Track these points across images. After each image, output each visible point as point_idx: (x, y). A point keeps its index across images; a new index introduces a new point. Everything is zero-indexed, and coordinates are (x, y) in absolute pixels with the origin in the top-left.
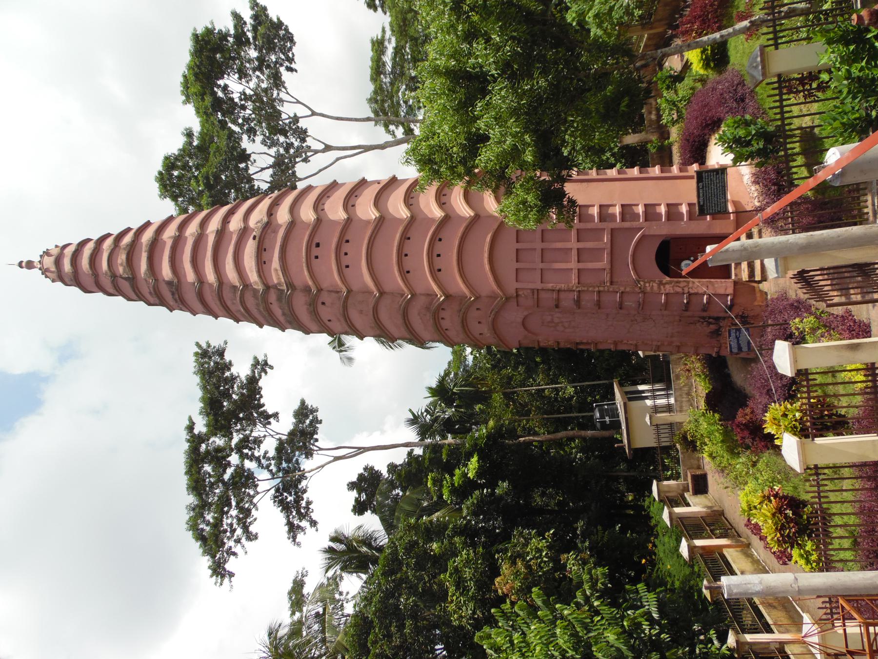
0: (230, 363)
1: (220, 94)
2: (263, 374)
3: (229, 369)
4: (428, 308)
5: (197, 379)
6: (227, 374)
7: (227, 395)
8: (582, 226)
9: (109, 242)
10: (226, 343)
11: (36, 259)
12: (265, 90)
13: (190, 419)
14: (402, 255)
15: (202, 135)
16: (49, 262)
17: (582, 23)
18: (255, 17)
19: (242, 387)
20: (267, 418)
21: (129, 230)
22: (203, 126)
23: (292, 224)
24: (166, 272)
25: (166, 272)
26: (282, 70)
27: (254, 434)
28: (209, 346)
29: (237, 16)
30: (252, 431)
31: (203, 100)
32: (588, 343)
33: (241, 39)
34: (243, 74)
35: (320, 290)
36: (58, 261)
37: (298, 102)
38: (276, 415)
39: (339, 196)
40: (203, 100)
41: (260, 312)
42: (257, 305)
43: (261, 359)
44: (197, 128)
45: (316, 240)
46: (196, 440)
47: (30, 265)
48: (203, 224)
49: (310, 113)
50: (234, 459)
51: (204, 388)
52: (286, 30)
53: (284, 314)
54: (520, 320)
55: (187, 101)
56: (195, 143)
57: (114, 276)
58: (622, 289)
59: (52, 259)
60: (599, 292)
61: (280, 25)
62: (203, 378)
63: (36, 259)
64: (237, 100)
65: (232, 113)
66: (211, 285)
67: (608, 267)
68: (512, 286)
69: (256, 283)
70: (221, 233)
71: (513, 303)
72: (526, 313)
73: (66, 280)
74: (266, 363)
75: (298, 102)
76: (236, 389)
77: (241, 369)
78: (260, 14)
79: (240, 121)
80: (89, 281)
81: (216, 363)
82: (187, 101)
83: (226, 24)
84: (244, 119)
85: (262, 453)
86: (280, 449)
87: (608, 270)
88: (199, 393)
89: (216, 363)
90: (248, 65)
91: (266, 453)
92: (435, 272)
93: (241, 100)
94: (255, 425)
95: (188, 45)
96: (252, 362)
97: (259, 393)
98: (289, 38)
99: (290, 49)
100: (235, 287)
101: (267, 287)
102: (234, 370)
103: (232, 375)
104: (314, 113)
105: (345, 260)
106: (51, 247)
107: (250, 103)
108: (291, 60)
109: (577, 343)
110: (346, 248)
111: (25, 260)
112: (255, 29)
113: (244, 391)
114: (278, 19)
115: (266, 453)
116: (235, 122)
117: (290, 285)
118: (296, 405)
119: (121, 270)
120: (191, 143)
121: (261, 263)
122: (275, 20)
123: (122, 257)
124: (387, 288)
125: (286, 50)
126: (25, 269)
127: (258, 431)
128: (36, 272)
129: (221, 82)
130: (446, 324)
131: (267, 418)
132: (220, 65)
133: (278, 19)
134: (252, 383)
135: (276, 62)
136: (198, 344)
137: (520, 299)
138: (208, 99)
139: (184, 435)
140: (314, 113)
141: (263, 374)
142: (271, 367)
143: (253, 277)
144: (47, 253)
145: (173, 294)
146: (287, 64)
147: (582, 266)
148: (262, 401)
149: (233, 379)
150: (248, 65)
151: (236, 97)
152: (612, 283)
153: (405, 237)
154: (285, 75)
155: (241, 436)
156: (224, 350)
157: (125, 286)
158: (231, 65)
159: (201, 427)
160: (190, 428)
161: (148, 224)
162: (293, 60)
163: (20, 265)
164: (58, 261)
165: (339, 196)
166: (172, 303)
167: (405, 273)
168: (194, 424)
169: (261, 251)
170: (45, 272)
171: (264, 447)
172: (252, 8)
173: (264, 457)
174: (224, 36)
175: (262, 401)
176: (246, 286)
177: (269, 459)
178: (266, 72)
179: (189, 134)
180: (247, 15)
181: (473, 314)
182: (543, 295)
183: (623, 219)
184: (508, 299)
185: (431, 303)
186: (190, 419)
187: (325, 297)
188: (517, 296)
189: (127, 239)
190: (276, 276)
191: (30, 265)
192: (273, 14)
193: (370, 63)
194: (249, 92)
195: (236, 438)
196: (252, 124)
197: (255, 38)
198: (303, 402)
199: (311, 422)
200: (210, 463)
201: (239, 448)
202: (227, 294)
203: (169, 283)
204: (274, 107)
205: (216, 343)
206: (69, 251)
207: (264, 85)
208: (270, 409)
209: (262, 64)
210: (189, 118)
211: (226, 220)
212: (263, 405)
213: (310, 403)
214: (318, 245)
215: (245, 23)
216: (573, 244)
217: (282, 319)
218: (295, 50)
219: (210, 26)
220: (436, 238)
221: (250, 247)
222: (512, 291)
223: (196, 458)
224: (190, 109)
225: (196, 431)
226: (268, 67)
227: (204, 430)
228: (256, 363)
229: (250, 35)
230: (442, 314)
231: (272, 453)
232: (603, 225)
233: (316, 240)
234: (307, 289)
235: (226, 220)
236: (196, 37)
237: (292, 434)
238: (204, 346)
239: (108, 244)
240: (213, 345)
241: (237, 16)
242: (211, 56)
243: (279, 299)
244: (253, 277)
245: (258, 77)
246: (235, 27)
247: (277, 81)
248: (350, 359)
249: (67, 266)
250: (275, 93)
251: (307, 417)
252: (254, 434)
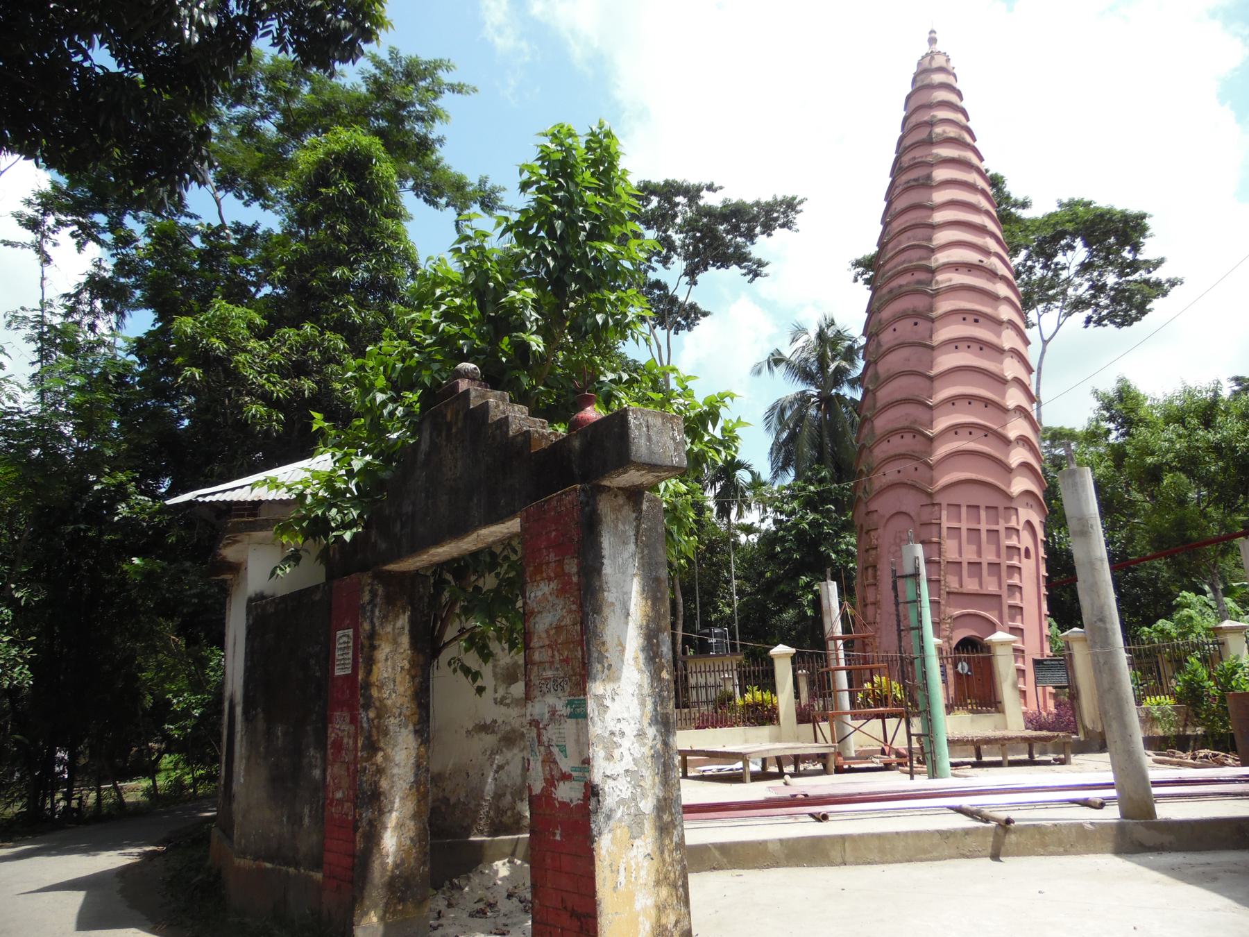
0: (769, 235)
1: (1063, 242)
2: (744, 271)
3: (763, 233)
4: (915, 422)
5: (766, 198)
6: (758, 230)
7: (735, 229)
8: (1004, 568)
9: (959, 117)
10: (797, 231)
11: (938, 47)
12: (1064, 292)
13: (721, 188)
14: (970, 398)
15: (1019, 220)
16: (939, 61)
17: (1181, 606)
18: (1158, 284)
19: (737, 247)
20: (691, 273)
21: (975, 140)
22: (1033, 221)
23: (995, 298)
24: (940, 174)
25: (940, 174)
26: (1089, 312)
27: (675, 257)
28: (797, 212)
29: (1159, 263)
30: (679, 255)
31: (1069, 221)
32: (875, 577)
33: (1134, 266)
34: (1085, 267)
35: (933, 320)
36: (942, 70)
37: (1059, 326)
38: (695, 283)
39: (1019, 345)
40: (1069, 221)
41: (904, 262)
42: (911, 261)
43: (764, 270)
44: (1025, 214)
45: (981, 320)
46: (693, 193)
47: (932, 41)
48: (987, 213)
49: (1046, 338)
50: (651, 234)
51: (757, 204)
52: (1137, 319)
53: (901, 286)
54: (904, 509)
55: (1061, 205)
56: (1013, 210)
57: (931, 124)
58: (943, 602)
59: (944, 64)
60: (939, 581)
61: (1142, 311)
62: (768, 204)
63: (938, 47)
64: (1056, 260)
65: (1039, 255)
66: (930, 217)
67: (965, 591)
68: (943, 499)
69: (937, 260)
70: (982, 230)
71: (925, 500)
72: (912, 514)
73: (922, 76)
74: (756, 275)
75: (1059, 326)
76: (739, 239)
77: (761, 247)
78: (1158, 289)
79: (1029, 263)
80: (922, 98)
81: (776, 219)
82: (1061, 205)
83: (1148, 252)
84: (1032, 268)
85: (654, 264)
86: (658, 284)
87: (960, 590)
88: (749, 200)
89: (776, 219)
90: (1096, 274)
91: (654, 270)
92: (955, 429)
93: (1057, 264)
94: (685, 259)
95: (1133, 208)
96: (765, 259)
97: (722, 266)
98: (1127, 321)
99: (1113, 322)
100: (930, 239)
101: (933, 271)
102: (761, 239)
103: (756, 236)
104: (1045, 343)
105: (963, 345)
106: (952, 64)
107: (1050, 274)
108: (1099, 322)
109: (875, 567)
110: (975, 347)
111: (937, 36)
112: (1146, 282)
113: (731, 250)
114: (1150, 310)
115: (654, 270)
116: (1029, 257)
117: (937, 293)
118: (703, 307)
119: (938, 130)
120: (1013, 206)
121: (957, 266)
122: (1148, 307)
123: (952, 132)
124: (937, 384)
125: (1111, 317)
126: (927, 36)
127: (679, 264)
128: (926, 49)
129: (1079, 243)
130: (895, 440)
131: (691, 273)
132: (1100, 242)
133: (1150, 310)
134: (740, 258)
135: (1097, 305)
136: (801, 202)
137: (929, 509)
138: (1070, 227)
139: (706, 181)
140: (1045, 343)
141: (744, 271)
142: (751, 281)
143: (942, 257)
144: (948, 60)
145: (915, 180)
146: (1095, 317)
147: (965, 565)
148: (712, 270)
149: (751, 237)
150: (1096, 274)
151: (1060, 258)
152: (948, 593)
153: (987, 402)
154: (1080, 317)
155: (678, 243)
156: (790, 228)
157: (922, 134)
158: (1107, 253)
159: (709, 200)
160: (710, 188)
161: (981, 159)
162: (1099, 324)
163: (932, 32)
164: (942, 70)
165: (1019, 345)
166: (904, 178)
167: (952, 400)
168: (715, 191)
169: (969, 267)
170: (931, 55)
171: (659, 266)
172: (1168, 281)
173: (650, 267)
174: (1136, 248)
175: (712, 270)
176: (932, 251)
177: (646, 272)
178: (1087, 296)
179: (1025, 205)
180: (1159, 275)
181: (909, 465)
182: (935, 529)
183: (1011, 607)
184: (930, 495)
185: (922, 425)
186: (721, 188)
187: (923, 325)
188: (933, 505)
189: (968, 139)
190: (944, 279)
191: (932, 41)
192: (1156, 304)
193: (1067, 427)
194: (1064, 275)
195: (677, 238)
196: (1024, 276)
197: (1136, 281)
198: (705, 314)
199: (679, 323)
200: (659, 206)
201: (667, 242)
202: (920, 232)
203: (929, 177)
204: (1040, 301)
205: (799, 220)
206: (950, 80)
207: (1070, 291)
208: (700, 278)
209: (1098, 288)
210: (1041, 207)
211: (993, 235)
212: (706, 269)
213: (703, 321)
214: (976, 321)
215: (1150, 272)
216: (989, 556)
217: (894, 284)
218: (1111, 327)
219: (1148, 233)
220: (987, 431)
221: (973, 257)
222: (937, 500)
223: (669, 191)
224: (1054, 208)
225: (704, 193)
226: (1094, 296)
227: (701, 203)
228: (760, 264)
229: (1136, 276)
230: (908, 437)
231: (652, 276)
232: (1005, 587)
233: (981, 320)
234: (931, 309)
235: (993, 235)
236: (1143, 216)
237: (673, 300)
238: (799, 208)
239: (959, 117)
240: (798, 216)
241: (1159, 263)
242: (1112, 233)
243: (919, 282)
244: (942, 257)
245: (1081, 285)
246: (1146, 262)
247: (1079, 305)
248: (759, 372)
249: (938, 78)
250: (1060, 304)
251: (685, 319)
252: (675, 258)
